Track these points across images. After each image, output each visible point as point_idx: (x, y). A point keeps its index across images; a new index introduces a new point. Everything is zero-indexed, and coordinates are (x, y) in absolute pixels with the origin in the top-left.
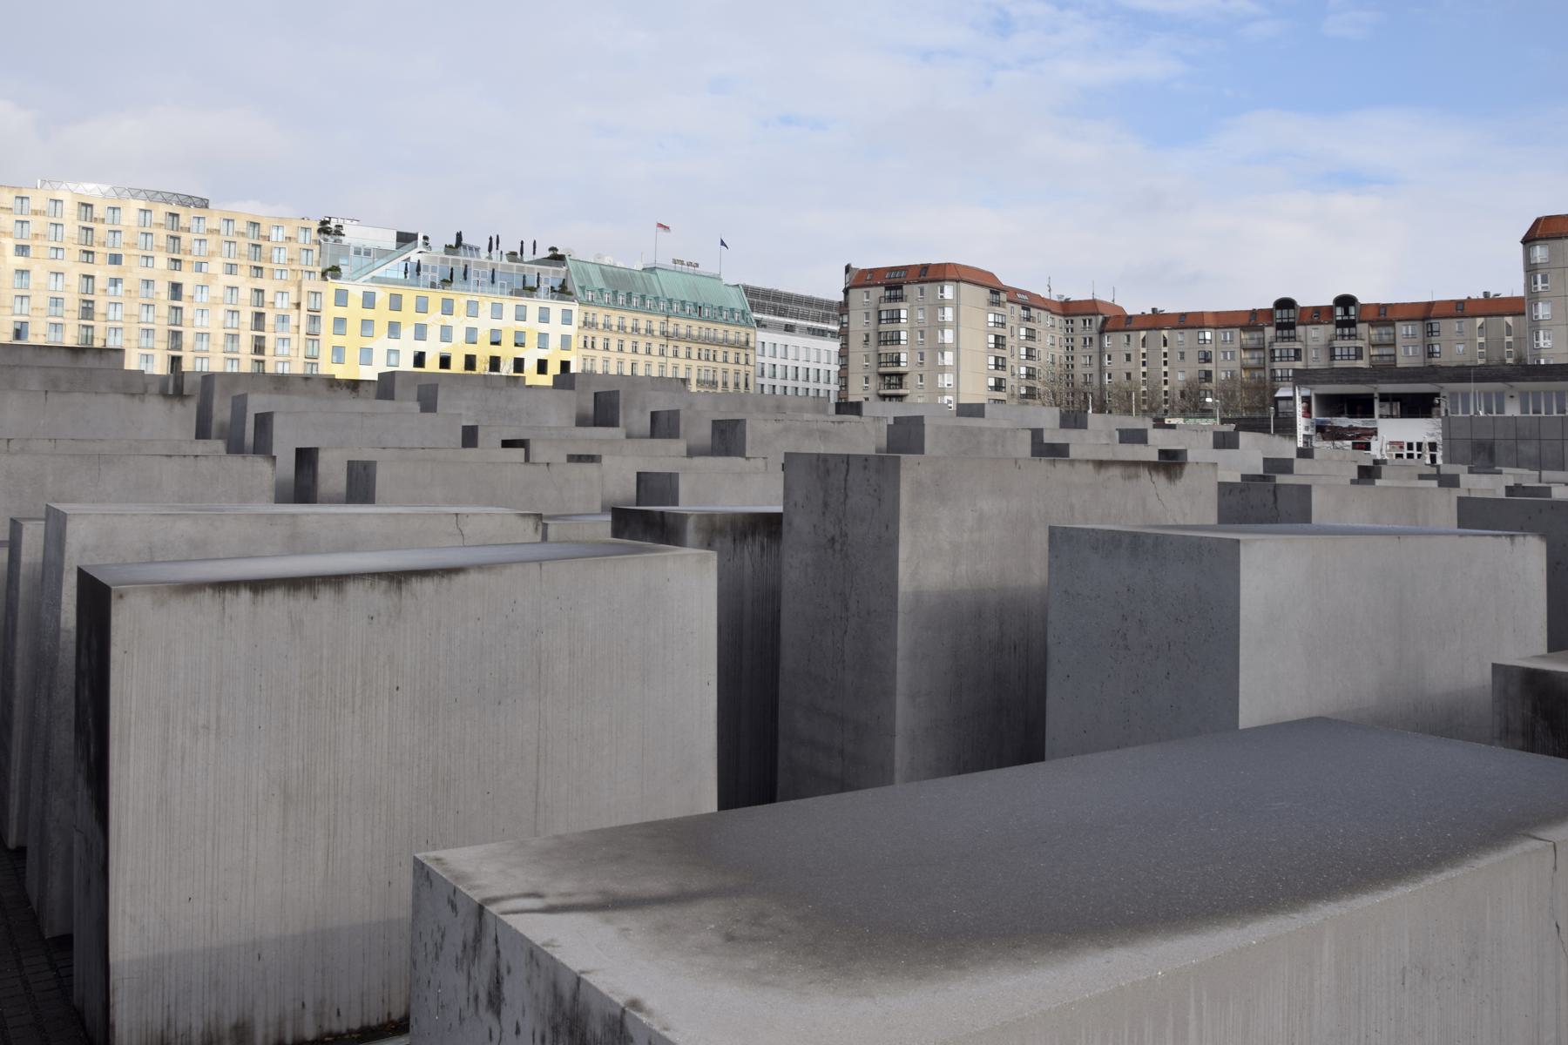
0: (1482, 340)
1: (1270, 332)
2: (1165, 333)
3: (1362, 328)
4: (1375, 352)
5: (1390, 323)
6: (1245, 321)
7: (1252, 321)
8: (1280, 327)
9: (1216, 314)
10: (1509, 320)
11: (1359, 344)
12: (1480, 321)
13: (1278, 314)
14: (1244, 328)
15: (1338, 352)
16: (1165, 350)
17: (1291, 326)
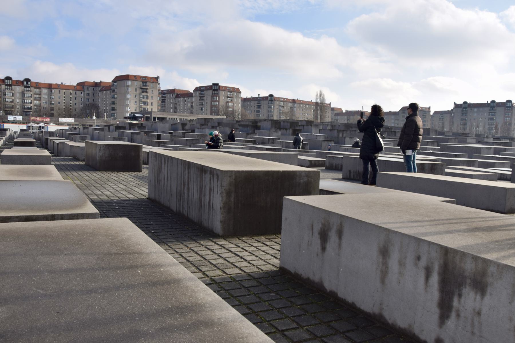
0: (64, 96)
3: (32, 89)
4: (35, 96)
8: (7, 85)
10: (71, 91)
11: (32, 93)
12: (64, 91)
17: (10, 85)
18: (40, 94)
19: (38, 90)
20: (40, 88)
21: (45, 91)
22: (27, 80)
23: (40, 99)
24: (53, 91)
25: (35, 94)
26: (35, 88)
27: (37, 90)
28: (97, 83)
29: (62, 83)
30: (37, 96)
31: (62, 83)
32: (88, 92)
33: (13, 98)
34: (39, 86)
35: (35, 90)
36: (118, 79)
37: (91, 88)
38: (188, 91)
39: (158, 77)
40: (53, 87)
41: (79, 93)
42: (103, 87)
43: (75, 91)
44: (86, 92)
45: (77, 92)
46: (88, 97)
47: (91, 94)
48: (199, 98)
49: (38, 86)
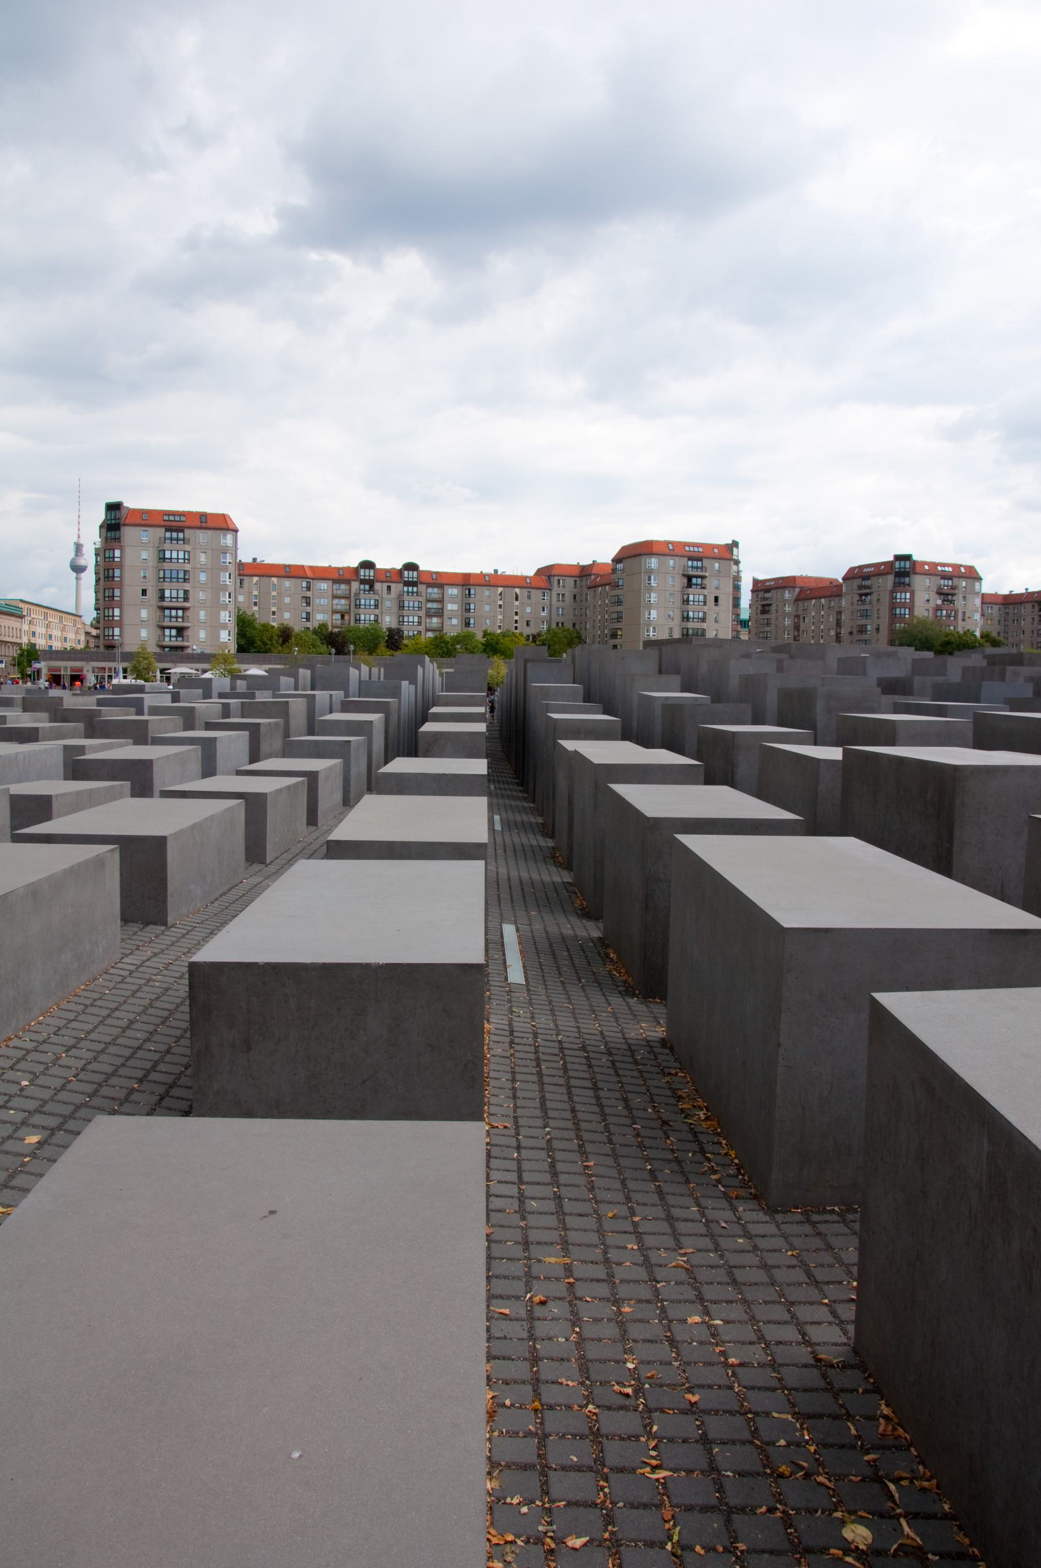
0: (500, 603)
1: (355, 585)
2: (274, 580)
3: (422, 588)
4: (430, 605)
5: (441, 586)
6: (336, 576)
7: (339, 577)
8: (363, 582)
9: (311, 567)
10: (517, 590)
11: (420, 599)
12: (500, 589)
13: (362, 572)
14: (335, 581)
15: (406, 604)
16: (274, 593)
18: (441, 601)
19: (436, 590)
20: (441, 586)
21: (453, 591)
22: (411, 567)
23: (440, 613)
24: (472, 591)
25: (428, 601)
26: (429, 585)
27: (434, 592)
28: (583, 567)
29: (496, 571)
30: (435, 605)
31: (496, 571)
32: (561, 591)
33: (377, 612)
34: (440, 581)
35: (430, 590)
36: (633, 555)
37: (570, 582)
38: (832, 581)
39: (735, 544)
40: (472, 581)
41: (536, 594)
42: (597, 575)
43: (525, 591)
44: (556, 590)
45: (534, 592)
46: (560, 604)
47: (569, 597)
48: (857, 598)
49: (439, 581)
